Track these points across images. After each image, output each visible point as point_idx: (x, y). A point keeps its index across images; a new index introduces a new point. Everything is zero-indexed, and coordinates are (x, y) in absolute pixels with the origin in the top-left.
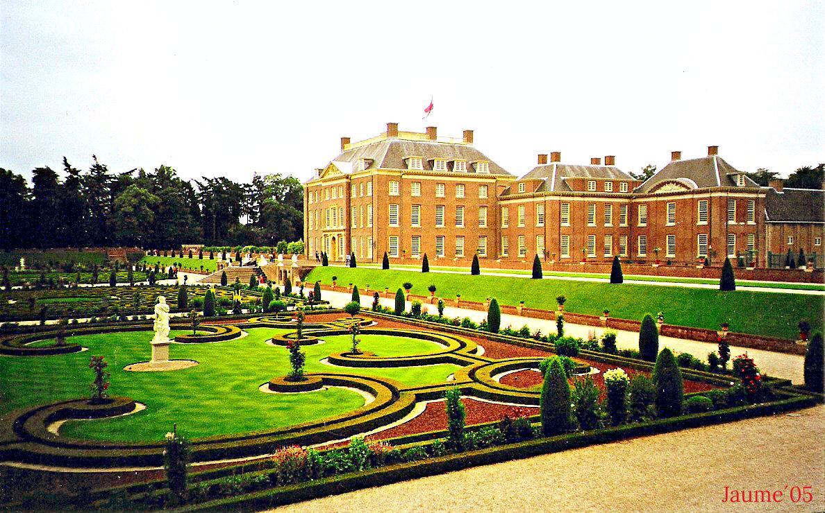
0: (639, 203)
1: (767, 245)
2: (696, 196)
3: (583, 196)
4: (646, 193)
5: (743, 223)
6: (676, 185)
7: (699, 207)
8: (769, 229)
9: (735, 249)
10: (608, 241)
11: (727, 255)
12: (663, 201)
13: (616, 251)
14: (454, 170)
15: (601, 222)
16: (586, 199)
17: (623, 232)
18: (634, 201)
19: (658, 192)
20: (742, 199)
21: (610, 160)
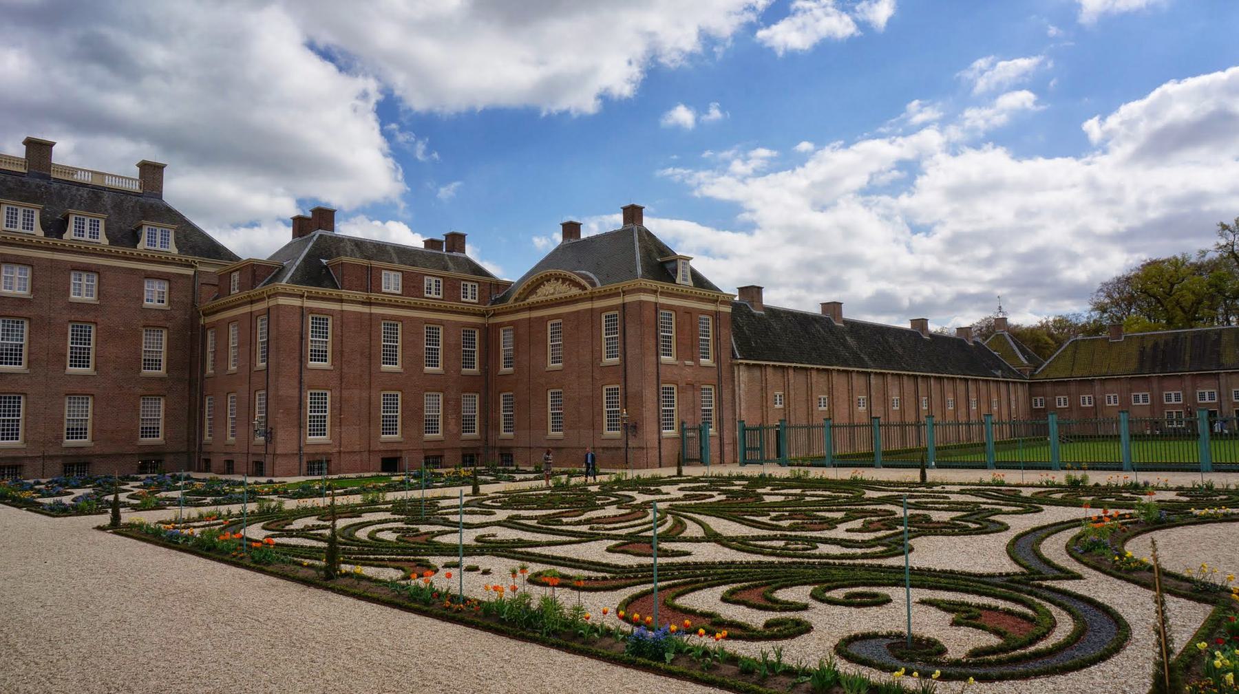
2: (598, 304)
3: (369, 303)
6: (563, 283)
7: (604, 328)
8: (743, 375)
9: (675, 417)
10: (434, 406)
11: (659, 432)
12: (542, 318)
13: (453, 427)
14: (70, 234)
15: (414, 363)
16: (376, 310)
17: (470, 384)
18: (492, 321)
19: (533, 299)
20: (688, 312)
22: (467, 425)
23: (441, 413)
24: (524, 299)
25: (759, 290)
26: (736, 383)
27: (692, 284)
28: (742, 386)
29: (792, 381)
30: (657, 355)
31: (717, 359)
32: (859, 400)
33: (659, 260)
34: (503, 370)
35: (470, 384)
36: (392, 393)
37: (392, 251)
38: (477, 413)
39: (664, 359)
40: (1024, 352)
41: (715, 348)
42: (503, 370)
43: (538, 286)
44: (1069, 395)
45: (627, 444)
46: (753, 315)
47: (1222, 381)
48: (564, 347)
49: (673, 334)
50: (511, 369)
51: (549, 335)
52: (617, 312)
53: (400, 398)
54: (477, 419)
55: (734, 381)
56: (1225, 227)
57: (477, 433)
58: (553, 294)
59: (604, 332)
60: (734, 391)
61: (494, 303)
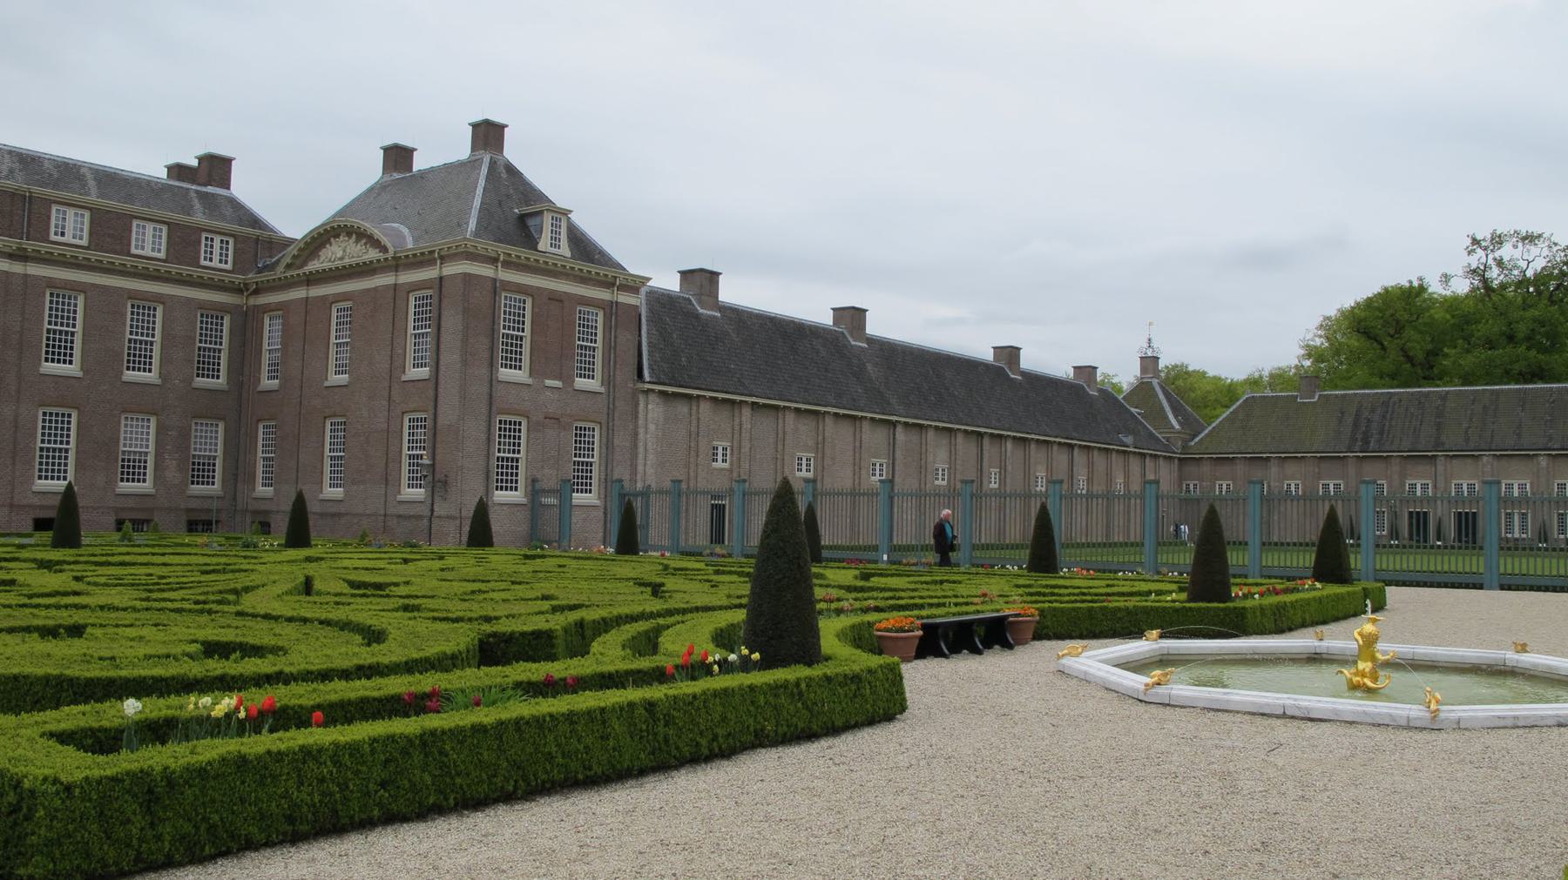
0: (267, 309)
1: (640, 468)
2: (407, 277)
4: (280, 271)
5: (558, 384)
8: (653, 412)
9: (521, 471)
12: (324, 298)
13: (172, 474)
15: (103, 362)
16: (34, 270)
17: (208, 407)
18: (253, 301)
19: (314, 266)
20: (556, 298)
21: (216, 168)
22: (201, 472)
23: (152, 449)
24: (304, 264)
25: (713, 276)
26: (641, 422)
27: (568, 254)
28: (652, 427)
29: (746, 426)
30: (491, 365)
31: (608, 381)
32: (874, 465)
33: (516, 211)
34: (267, 383)
35: (208, 407)
36: (61, 410)
37: (89, 176)
38: (220, 453)
39: (505, 374)
40: (1177, 410)
41: (606, 362)
42: (267, 383)
43: (322, 246)
44: (1233, 479)
45: (432, 511)
46: (697, 316)
47: (1440, 468)
48: (352, 348)
49: (527, 333)
50: (277, 381)
51: (334, 327)
52: (429, 292)
53: (74, 420)
54: (218, 462)
55: (637, 417)
56: (1475, 242)
57: (216, 488)
58: (342, 259)
59: (411, 324)
60: (636, 434)
61: (260, 271)
